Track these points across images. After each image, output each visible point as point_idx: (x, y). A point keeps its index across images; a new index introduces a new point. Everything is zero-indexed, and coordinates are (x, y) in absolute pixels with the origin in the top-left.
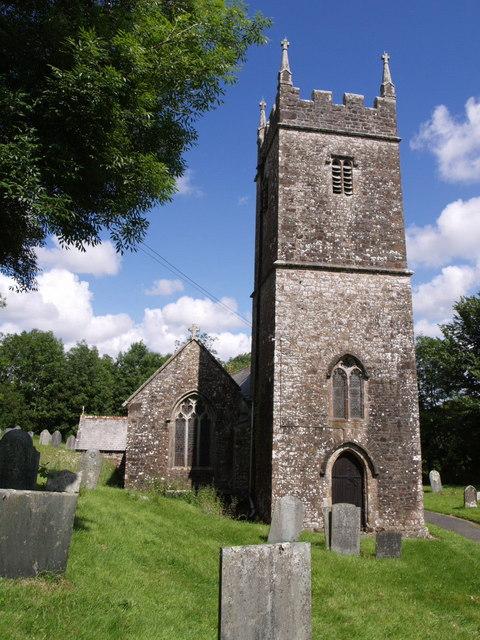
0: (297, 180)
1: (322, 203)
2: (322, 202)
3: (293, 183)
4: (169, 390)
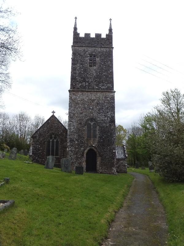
0: (77, 63)
1: (85, 70)
2: (85, 70)
3: (76, 64)
4: (45, 132)
